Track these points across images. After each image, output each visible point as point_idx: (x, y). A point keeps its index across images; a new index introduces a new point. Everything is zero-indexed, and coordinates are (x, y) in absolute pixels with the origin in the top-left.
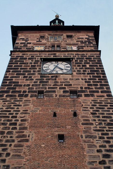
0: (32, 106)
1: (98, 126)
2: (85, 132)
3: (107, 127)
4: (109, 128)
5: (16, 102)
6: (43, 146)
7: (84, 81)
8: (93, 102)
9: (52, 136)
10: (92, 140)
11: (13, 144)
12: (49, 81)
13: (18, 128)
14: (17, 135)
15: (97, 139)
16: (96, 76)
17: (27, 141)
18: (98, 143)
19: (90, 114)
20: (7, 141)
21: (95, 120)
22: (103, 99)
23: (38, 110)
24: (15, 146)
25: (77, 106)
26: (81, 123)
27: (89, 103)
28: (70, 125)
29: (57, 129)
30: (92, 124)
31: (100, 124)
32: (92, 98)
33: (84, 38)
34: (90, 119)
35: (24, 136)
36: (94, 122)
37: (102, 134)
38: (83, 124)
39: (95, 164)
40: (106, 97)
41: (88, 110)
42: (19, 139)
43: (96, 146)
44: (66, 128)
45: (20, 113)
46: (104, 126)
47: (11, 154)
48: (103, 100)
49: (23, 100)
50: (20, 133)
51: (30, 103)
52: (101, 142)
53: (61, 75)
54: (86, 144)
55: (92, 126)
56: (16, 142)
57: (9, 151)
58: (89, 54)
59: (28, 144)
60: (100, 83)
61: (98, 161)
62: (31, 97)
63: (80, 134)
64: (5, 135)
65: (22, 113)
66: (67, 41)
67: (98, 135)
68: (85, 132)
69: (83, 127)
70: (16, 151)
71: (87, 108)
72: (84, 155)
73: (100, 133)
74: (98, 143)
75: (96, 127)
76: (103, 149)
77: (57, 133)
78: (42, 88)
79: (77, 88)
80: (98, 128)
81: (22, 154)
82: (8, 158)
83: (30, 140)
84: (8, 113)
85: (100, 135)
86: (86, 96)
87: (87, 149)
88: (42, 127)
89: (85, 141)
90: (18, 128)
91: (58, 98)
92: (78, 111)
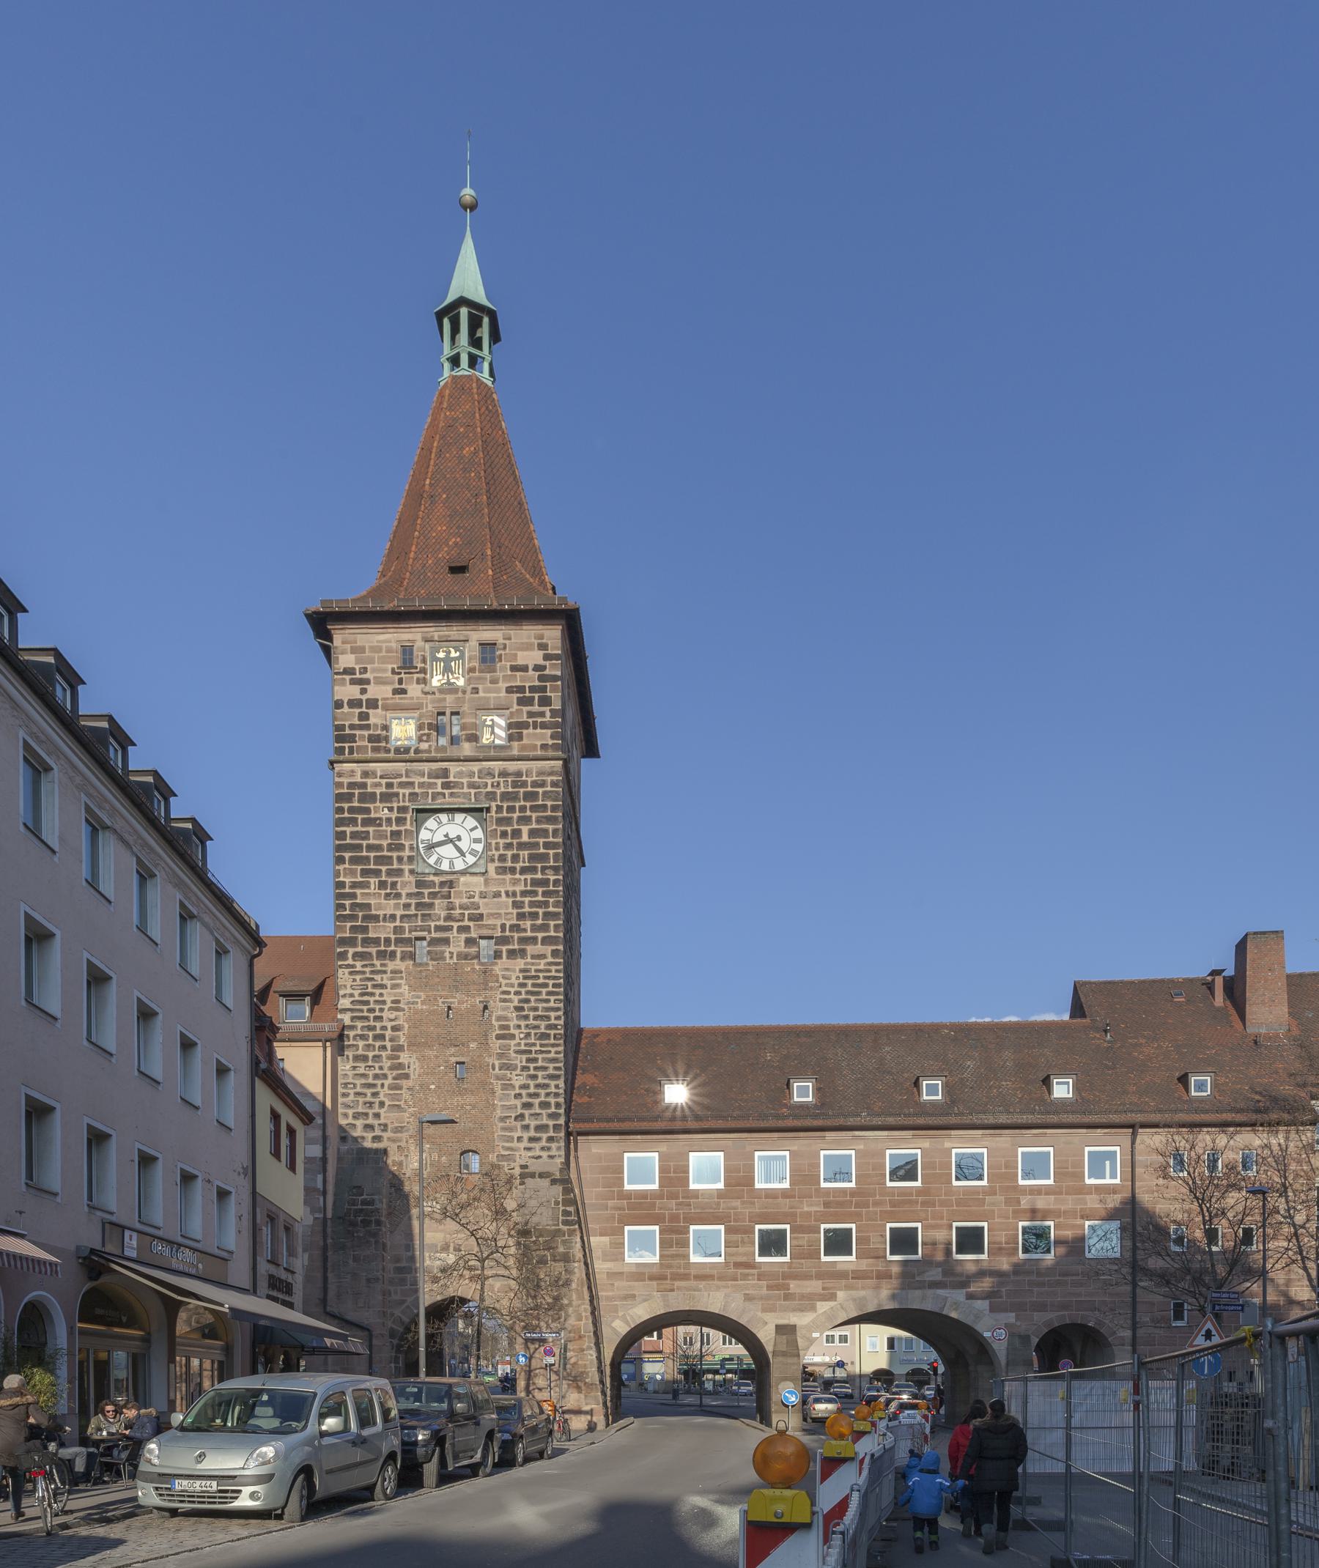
0: (407, 987)
1: (523, 1042)
2: (500, 1056)
3: (538, 1042)
4: (541, 1045)
5: (375, 977)
6: (433, 1087)
7: (510, 900)
8: (521, 975)
9: (446, 1067)
10: (509, 1075)
11: (387, 1083)
12: (437, 902)
13: (389, 1048)
14: (389, 1064)
15: (518, 1072)
16: (539, 879)
17: (407, 1076)
18: (518, 1080)
19: (512, 1009)
20: (376, 1077)
21: (519, 1027)
23: (419, 1000)
24: (391, 1088)
25: (491, 988)
26: (494, 1034)
27: (513, 980)
28: (475, 1040)
29: (453, 1050)
30: (512, 1037)
31: (528, 1035)
32: (520, 963)
33: (530, 668)
34: (512, 1024)
35: (400, 1066)
36: (516, 1032)
37: (528, 1060)
38: (499, 1037)
40: (550, 959)
41: (510, 1001)
42: (395, 1073)
43: (513, 1087)
44: (468, 1047)
45: (386, 1007)
46: (533, 1041)
47: (387, 1103)
48: (542, 967)
49: (389, 969)
50: (393, 1059)
51: (402, 978)
53: (462, 879)
54: (500, 1082)
55: (513, 1043)
57: (382, 1098)
59: (410, 1083)
60: (544, 910)
62: (403, 959)
63: (491, 1061)
64: (370, 1063)
65: (390, 1009)
66: (480, 687)
67: (521, 1062)
68: (500, 1056)
69: (498, 1045)
70: (392, 1097)
71: (509, 993)
72: (494, 1104)
73: (524, 1057)
74: (518, 1080)
75: (519, 1044)
76: (524, 1092)
79: (493, 927)
80: (523, 1047)
83: (412, 1076)
84: (365, 1008)
85: (524, 1064)
87: (499, 1092)
88: (427, 1045)
89: (498, 1078)
90: (389, 1048)
91: (455, 964)
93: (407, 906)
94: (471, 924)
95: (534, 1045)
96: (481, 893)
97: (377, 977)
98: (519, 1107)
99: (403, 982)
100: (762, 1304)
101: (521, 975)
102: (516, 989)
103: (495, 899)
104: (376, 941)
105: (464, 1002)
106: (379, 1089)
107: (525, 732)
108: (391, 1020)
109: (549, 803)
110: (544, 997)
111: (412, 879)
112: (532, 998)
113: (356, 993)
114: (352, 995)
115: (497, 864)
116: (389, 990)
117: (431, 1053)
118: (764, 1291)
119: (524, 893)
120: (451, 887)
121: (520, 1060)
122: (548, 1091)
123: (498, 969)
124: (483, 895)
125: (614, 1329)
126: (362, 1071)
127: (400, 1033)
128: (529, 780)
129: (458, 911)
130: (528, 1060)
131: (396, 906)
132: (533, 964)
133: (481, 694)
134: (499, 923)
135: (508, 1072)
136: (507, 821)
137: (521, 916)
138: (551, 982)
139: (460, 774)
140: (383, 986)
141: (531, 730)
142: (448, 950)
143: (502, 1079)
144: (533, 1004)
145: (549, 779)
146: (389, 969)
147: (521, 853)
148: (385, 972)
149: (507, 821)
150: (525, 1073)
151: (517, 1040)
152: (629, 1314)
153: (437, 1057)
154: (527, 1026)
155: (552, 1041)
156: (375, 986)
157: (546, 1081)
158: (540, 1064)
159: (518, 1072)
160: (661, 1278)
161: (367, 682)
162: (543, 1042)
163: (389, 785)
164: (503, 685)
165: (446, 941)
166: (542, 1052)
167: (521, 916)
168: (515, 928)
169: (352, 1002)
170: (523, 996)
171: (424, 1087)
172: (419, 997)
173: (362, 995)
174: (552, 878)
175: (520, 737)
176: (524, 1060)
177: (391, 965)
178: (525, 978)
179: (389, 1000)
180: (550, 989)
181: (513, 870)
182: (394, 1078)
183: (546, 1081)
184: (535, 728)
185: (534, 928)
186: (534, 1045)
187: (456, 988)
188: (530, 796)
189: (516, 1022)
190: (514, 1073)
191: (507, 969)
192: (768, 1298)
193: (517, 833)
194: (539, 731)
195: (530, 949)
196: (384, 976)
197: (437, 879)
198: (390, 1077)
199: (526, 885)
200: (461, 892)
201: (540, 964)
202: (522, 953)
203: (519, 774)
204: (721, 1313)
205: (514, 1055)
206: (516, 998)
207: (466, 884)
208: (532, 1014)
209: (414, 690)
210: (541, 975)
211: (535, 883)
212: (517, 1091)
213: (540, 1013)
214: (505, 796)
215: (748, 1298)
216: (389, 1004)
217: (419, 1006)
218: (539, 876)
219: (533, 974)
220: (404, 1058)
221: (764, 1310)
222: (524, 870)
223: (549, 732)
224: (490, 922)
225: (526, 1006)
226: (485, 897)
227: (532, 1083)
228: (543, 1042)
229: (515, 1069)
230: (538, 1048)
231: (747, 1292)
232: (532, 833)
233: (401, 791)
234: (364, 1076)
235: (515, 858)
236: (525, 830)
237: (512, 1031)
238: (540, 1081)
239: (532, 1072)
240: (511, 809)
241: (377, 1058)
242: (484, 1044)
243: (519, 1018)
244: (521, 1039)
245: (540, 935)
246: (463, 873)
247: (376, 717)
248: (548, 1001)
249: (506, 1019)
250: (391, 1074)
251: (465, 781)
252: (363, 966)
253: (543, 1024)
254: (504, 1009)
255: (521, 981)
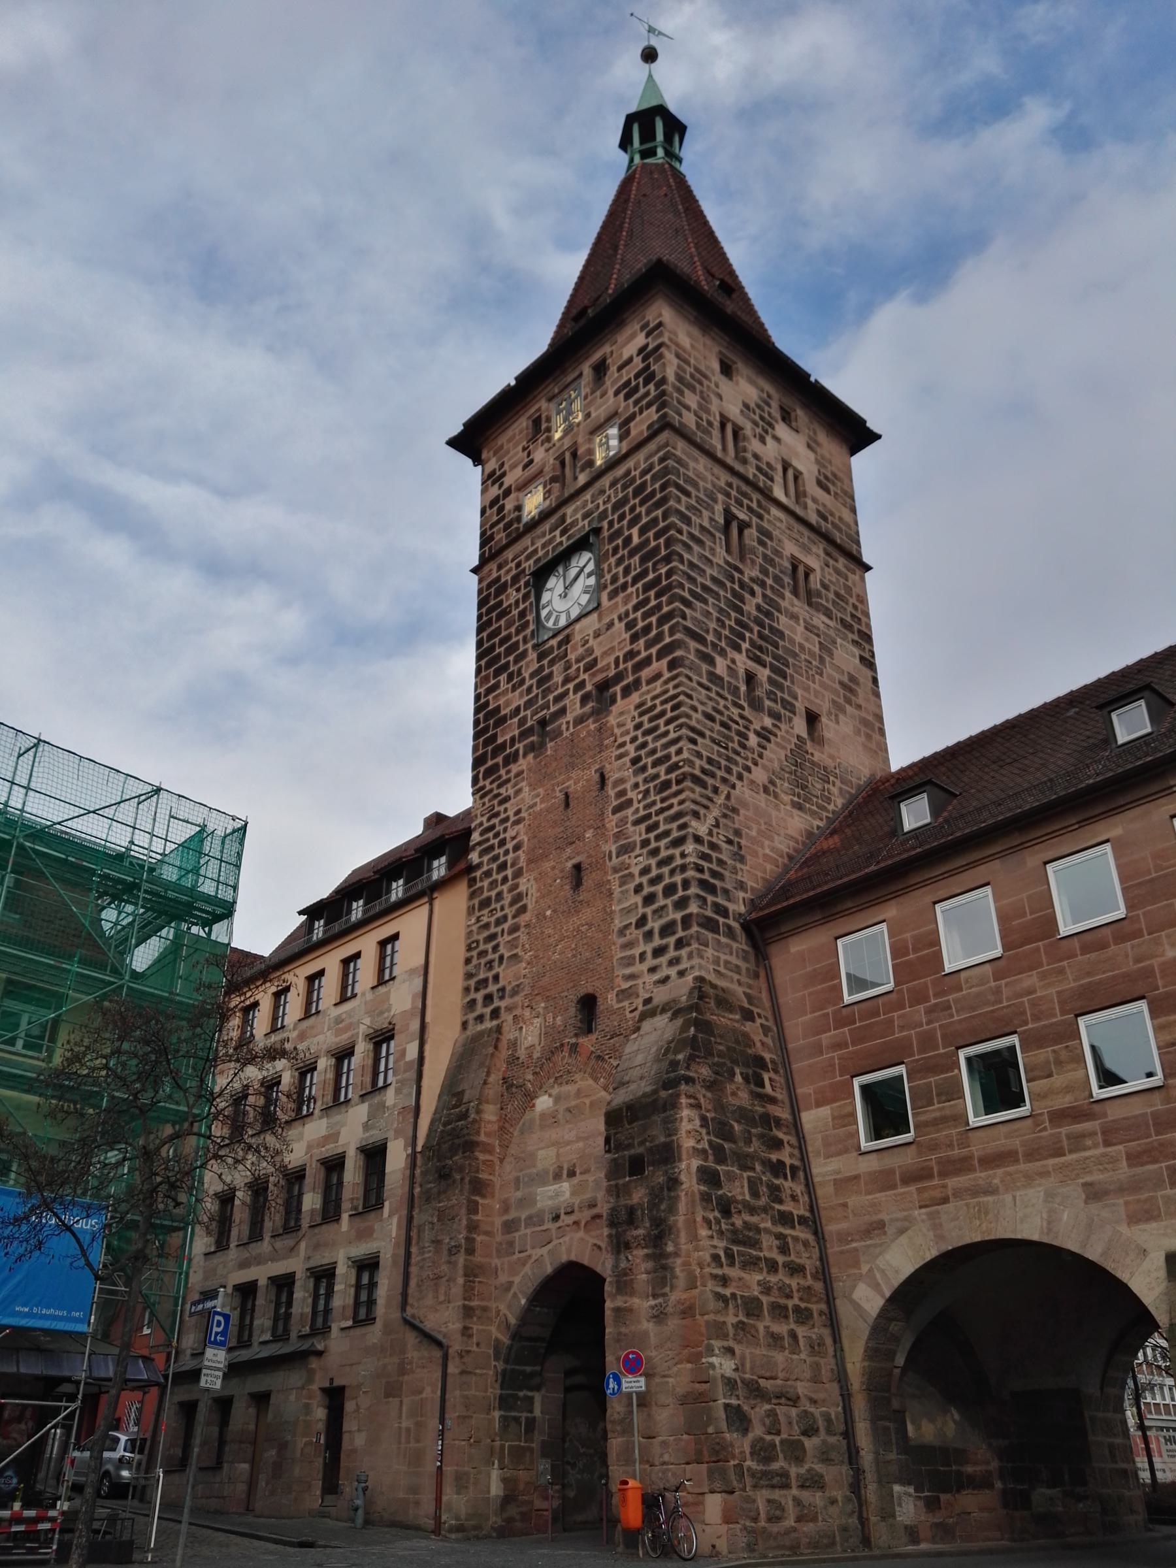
3: (658, 798)
7: (623, 624)
11: (506, 926)
12: (554, 668)
17: (524, 909)
18: (637, 861)
19: (629, 764)
20: (498, 922)
22: (658, 687)
23: (538, 800)
28: (590, 827)
29: (569, 850)
32: (635, 698)
37: (649, 829)
39: (628, 932)
40: (667, 675)
43: (631, 875)
46: (653, 798)
48: (658, 691)
52: (643, 861)
54: (617, 875)
56: (510, 922)
57: (502, 950)
58: (641, 456)
61: (633, 921)
64: (493, 906)
67: (640, 835)
68: (617, 836)
69: (614, 823)
72: (612, 912)
73: (643, 827)
74: (637, 861)
75: (637, 810)
76: (645, 880)
77: (569, 864)
78: (543, 708)
80: (642, 813)
81: (519, 951)
82: (503, 967)
83: (530, 907)
85: (644, 836)
86: (626, 692)
87: (617, 890)
88: (545, 856)
92: (607, 766)
93: (529, 690)
94: (586, 676)
95: (654, 803)
96: (595, 632)
97: (502, 790)
98: (640, 905)
99: (524, 784)
100: (1127, 1203)
101: (636, 714)
102: (632, 734)
103: (609, 632)
104: (503, 746)
105: (580, 781)
106: (500, 939)
107: (632, 424)
108: (513, 838)
109: (657, 486)
110: (663, 729)
111: (535, 656)
112: (649, 738)
113: (484, 819)
114: (481, 824)
115: (610, 588)
116: (513, 801)
117: (547, 865)
118: (1124, 1171)
119: (636, 608)
120: (567, 643)
121: (637, 834)
122: (673, 865)
123: (612, 720)
124: (597, 634)
125: (856, 1306)
126: (485, 920)
127: (520, 852)
128: (637, 473)
129: (575, 667)
130: (649, 829)
131: (521, 696)
132: (648, 692)
133: (593, 415)
134: (612, 659)
135: (626, 856)
136: (618, 533)
137: (634, 638)
138: (668, 706)
139: (576, 511)
140: (507, 799)
141: (638, 418)
142: (564, 721)
143: (621, 870)
144: (651, 746)
145: (656, 459)
146: (512, 774)
147: (632, 561)
148: (508, 780)
149: (618, 533)
150: (645, 851)
151: (636, 805)
152: (879, 1269)
153: (553, 868)
154: (646, 781)
155: (674, 788)
156: (501, 803)
157: (670, 852)
158: (662, 828)
159: (638, 851)
160: (914, 1177)
161: (504, 475)
162: (664, 794)
163: (518, 565)
164: (611, 393)
165: (563, 711)
166: (662, 810)
167: (634, 638)
168: (630, 655)
169: (481, 834)
170: (641, 740)
171: (541, 916)
172: (538, 795)
173: (489, 819)
174: (663, 571)
175: (628, 432)
176: (643, 831)
177: (514, 768)
178: (641, 714)
179: (511, 813)
180: (669, 715)
181: (624, 587)
182: (514, 917)
183: (670, 852)
184: (641, 412)
185: (648, 646)
186: (654, 803)
187: (573, 766)
188: (638, 491)
189: (633, 781)
190: (633, 855)
191: (622, 714)
192: (1134, 1186)
193: (628, 540)
194: (645, 413)
195: (646, 673)
196: (509, 785)
197: (554, 642)
198: (510, 917)
199: (638, 596)
200: (576, 644)
201: (655, 689)
202: (637, 684)
203: (628, 472)
204: (1046, 1240)
205: (632, 829)
206: (631, 748)
207: (581, 631)
208: (650, 760)
209: (539, 455)
210: (657, 701)
211: (647, 588)
212: (637, 881)
213: (659, 755)
214: (616, 507)
215: (1094, 1193)
216: (512, 819)
217: (538, 808)
218: (651, 576)
219: (649, 704)
220: (524, 884)
221: (1133, 1219)
222: (635, 580)
223: (654, 408)
224: (604, 663)
225: (643, 752)
226: (599, 635)
227: (653, 862)
228: (664, 794)
229: (633, 850)
230: (659, 806)
231: (1088, 1179)
232: (642, 532)
233: (527, 564)
234: (487, 926)
235: (627, 571)
236: (635, 531)
237: (631, 794)
238: (664, 854)
239: (653, 845)
240: (622, 518)
241: (499, 896)
242: (600, 828)
243: (636, 773)
244: (639, 802)
245: (654, 651)
246: (578, 619)
247: (509, 504)
248: (667, 733)
249: (622, 781)
250: (509, 911)
251: (579, 516)
252: (491, 783)
253: (662, 769)
254: (620, 769)
255: (637, 720)
